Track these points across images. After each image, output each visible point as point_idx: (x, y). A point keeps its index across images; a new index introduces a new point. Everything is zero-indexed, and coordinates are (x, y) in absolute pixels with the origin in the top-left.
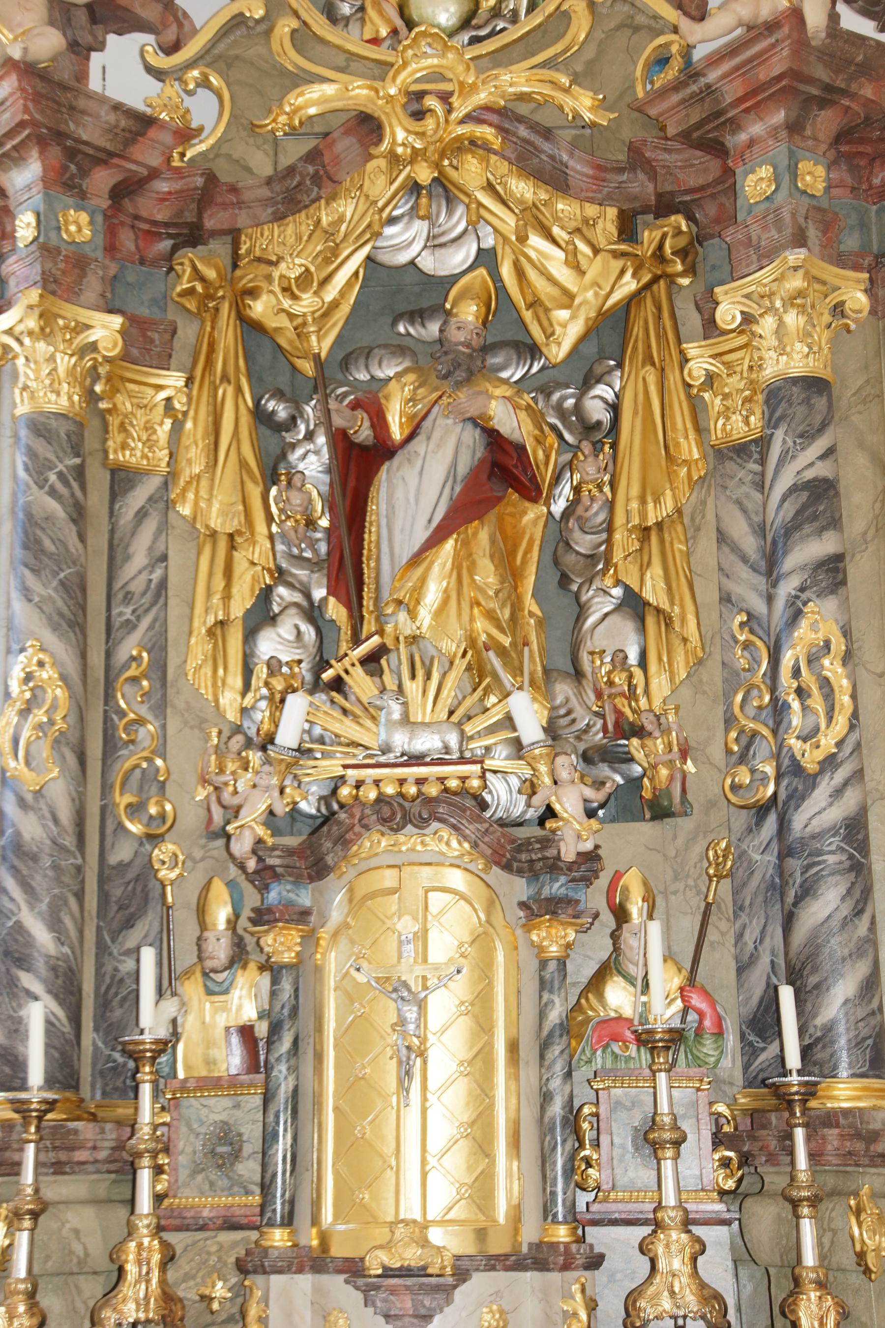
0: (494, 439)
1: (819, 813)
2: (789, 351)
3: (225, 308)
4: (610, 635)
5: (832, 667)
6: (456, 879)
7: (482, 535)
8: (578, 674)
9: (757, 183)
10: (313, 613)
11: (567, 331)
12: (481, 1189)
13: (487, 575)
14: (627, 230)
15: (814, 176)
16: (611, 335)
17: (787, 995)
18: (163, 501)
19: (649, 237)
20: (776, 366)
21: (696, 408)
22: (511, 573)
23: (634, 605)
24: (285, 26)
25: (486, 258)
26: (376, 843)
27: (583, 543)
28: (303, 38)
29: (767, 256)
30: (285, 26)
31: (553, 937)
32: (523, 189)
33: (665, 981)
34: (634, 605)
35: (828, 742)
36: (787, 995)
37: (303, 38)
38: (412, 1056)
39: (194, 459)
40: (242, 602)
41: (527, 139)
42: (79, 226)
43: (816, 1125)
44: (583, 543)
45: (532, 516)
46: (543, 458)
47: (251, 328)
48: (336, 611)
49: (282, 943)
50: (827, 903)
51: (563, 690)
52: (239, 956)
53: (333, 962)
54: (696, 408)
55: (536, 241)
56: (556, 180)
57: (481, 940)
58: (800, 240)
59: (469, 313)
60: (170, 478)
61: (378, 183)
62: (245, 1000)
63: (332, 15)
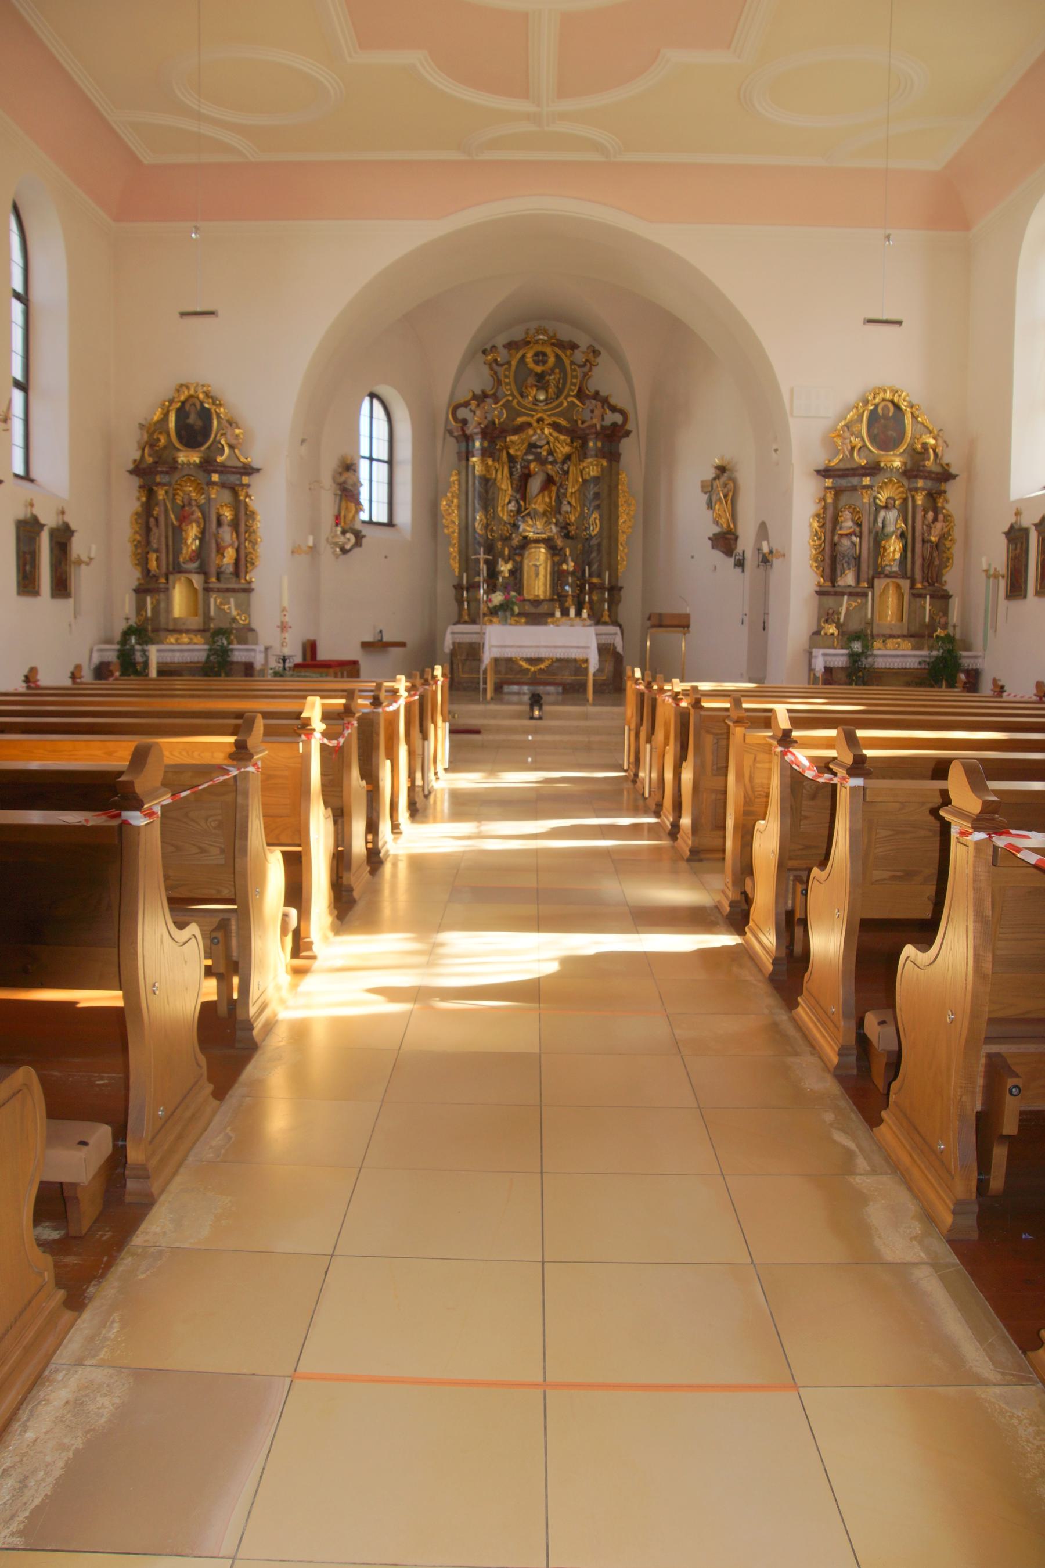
0: (548, 474)
1: (594, 542)
2: (593, 471)
3: (505, 452)
4: (566, 508)
5: (598, 521)
6: (543, 550)
7: (546, 493)
8: (560, 513)
9: (591, 444)
10: (517, 501)
11: (560, 457)
12: (545, 592)
13: (547, 500)
14: (572, 442)
15: (599, 444)
16: (568, 457)
17: (587, 568)
18: (494, 483)
19: (575, 444)
20: (592, 474)
21: (581, 472)
22: (550, 498)
23: (569, 503)
24: (515, 403)
25: (548, 443)
26: (533, 545)
27: (562, 491)
28: (519, 403)
29: (592, 457)
30: (515, 401)
31: (557, 559)
32: (555, 434)
33: (572, 564)
34: (569, 503)
35: (596, 532)
36: (587, 568)
37: (519, 403)
38: (537, 575)
39: (499, 476)
40: (507, 501)
41: (556, 426)
42: (486, 444)
43: (591, 584)
44: (562, 491)
45: (554, 489)
46: (557, 479)
47: (508, 454)
48: (522, 503)
49: (518, 559)
50: (594, 555)
51: (558, 516)
52: (509, 559)
53: (526, 562)
54: (581, 472)
55: (557, 444)
56: (560, 432)
57: (547, 558)
58: (596, 456)
59: (545, 453)
60: (495, 479)
61: (531, 432)
62: (509, 566)
63: (522, 396)
